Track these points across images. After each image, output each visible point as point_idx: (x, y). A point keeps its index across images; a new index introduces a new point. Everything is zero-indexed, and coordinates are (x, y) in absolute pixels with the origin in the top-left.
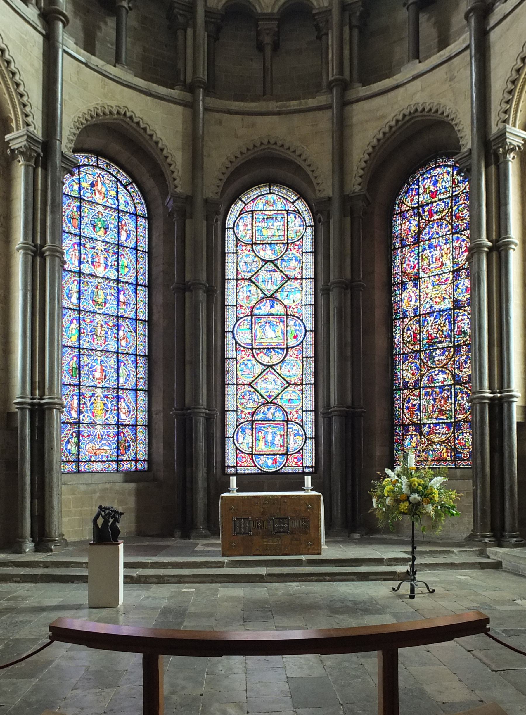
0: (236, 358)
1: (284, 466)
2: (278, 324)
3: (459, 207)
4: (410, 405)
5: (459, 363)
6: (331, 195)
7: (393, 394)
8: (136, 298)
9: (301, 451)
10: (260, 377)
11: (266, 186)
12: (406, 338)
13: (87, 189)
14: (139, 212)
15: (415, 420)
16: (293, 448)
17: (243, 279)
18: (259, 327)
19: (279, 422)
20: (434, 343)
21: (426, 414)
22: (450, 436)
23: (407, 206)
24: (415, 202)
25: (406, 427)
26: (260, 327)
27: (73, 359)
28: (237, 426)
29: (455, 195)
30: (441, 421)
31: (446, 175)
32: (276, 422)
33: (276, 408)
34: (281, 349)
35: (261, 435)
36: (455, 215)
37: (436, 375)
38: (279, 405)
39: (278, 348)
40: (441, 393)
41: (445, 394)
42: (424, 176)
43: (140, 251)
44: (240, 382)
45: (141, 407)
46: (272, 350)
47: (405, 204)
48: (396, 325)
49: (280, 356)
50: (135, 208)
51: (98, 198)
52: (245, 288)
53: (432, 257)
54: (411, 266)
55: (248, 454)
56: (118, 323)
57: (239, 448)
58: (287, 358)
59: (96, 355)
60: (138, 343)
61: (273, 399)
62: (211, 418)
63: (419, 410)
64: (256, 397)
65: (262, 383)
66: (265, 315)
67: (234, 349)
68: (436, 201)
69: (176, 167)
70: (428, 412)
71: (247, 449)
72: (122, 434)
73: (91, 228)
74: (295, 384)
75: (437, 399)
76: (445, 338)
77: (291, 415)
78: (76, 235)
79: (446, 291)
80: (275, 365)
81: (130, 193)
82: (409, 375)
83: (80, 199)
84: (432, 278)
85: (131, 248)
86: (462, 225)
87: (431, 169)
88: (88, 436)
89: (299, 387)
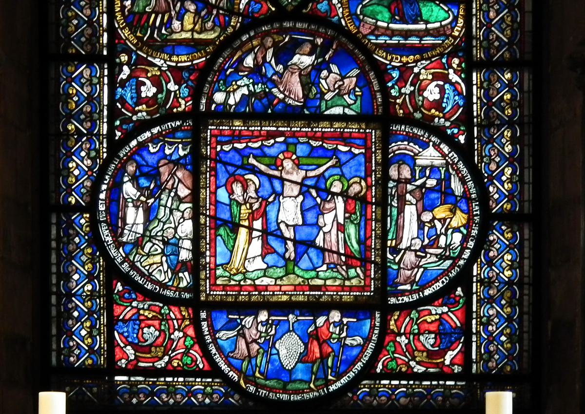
9: (459, 291)
33: (325, 47)
77: (408, 89)
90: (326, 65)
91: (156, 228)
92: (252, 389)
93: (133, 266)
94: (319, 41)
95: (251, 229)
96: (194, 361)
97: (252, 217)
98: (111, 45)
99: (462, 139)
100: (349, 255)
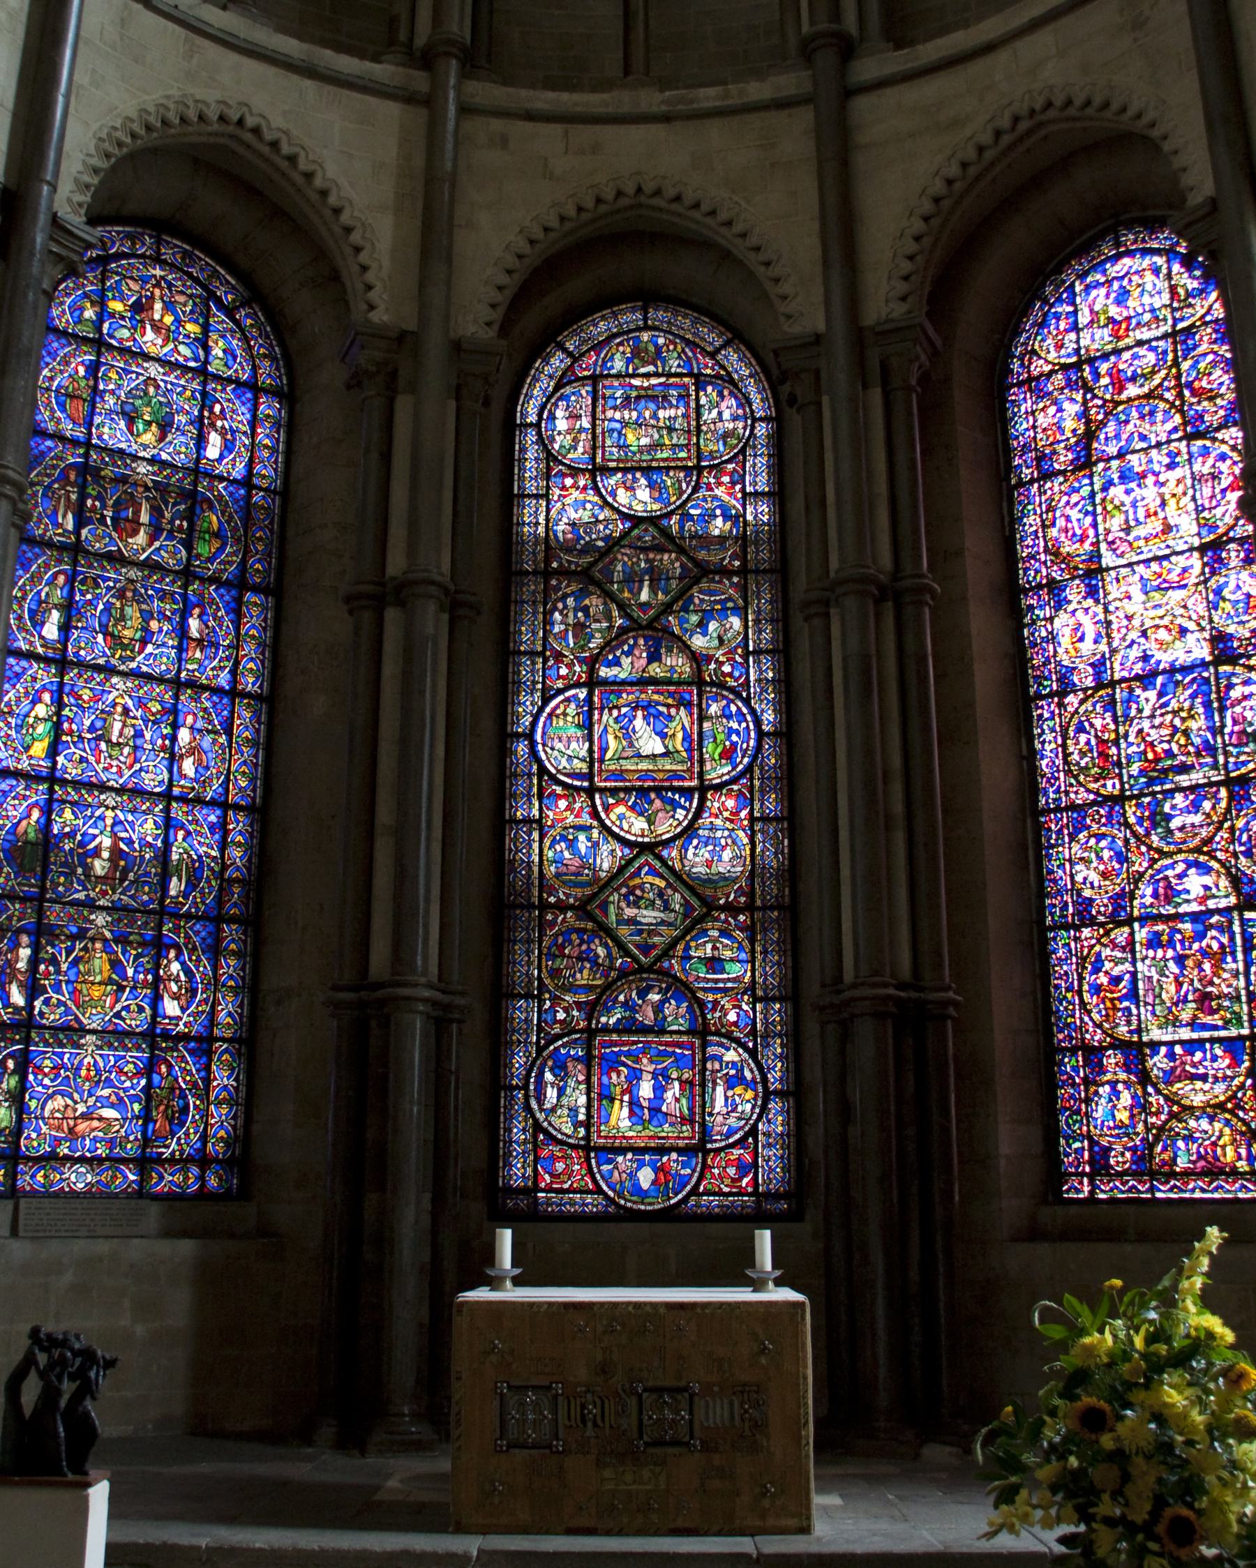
0: (539, 821)
1: (695, 1191)
2: (673, 711)
3: (1197, 362)
4: (1104, 980)
5: (1250, 837)
6: (821, 327)
7: (1046, 941)
8: (237, 630)
9: (750, 1140)
10: (615, 884)
11: (633, 310)
12: (1076, 757)
13: (123, 318)
14: (265, 380)
15: (1123, 1029)
16: (725, 1129)
17: (563, 573)
18: (611, 721)
19: (675, 1038)
20: (1165, 771)
21: (1158, 1008)
22: (1242, 1087)
23: (1047, 362)
24: (1070, 350)
25: (1093, 1055)
26: (616, 720)
27: (29, 816)
28: (540, 1050)
29: (1183, 330)
30: (1206, 1035)
31: (1149, 277)
32: (667, 1038)
33: (667, 989)
34: (681, 791)
35: (617, 1080)
36: (1189, 385)
37: (1180, 876)
38: (675, 977)
39: (674, 790)
40: (1200, 936)
41: (1213, 940)
42: (1089, 279)
43: (260, 489)
44: (552, 900)
45: (231, 977)
46: (653, 795)
47: (1040, 358)
48: (1040, 716)
49: (680, 814)
50: (255, 368)
51: (150, 340)
52: (570, 601)
53: (1134, 504)
54: (1074, 535)
55: (574, 1147)
56: (175, 706)
57: (545, 1124)
58: (706, 820)
59: (101, 805)
60: (233, 769)
61: (659, 959)
62: (451, 1021)
63: (1133, 995)
64: (601, 952)
65: (623, 904)
66: (632, 684)
67: (535, 790)
68: (1128, 348)
69: (375, 256)
70: (1163, 1002)
71: (568, 1129)
72: (164, 1069)
73: (122, 424)
74: (732, 909)
75: (1187, 957)
76: (1198, 754)
77: (717, 1014)
78: (75, 442)
79: (1185, 607)
80: (666, 843)
81: (242, 331)
82: (1094, 877)
83: (99, 344)
84: (1140, 569)
85: (235, 481)
86: (1213, 413)
87: (1104, 262)
88: (56, 1068)
89: (742, 918)
90: (667, 1000)
91: (565, 1101)
92: (622, 1202)
93: (550, 1124)
94: (664, 986)
95: (622, 1101)
96: (587, 1184)
97: (623, 1093)
98: (539, 988)
99: (751, 1045)
100: (682, 1117)
